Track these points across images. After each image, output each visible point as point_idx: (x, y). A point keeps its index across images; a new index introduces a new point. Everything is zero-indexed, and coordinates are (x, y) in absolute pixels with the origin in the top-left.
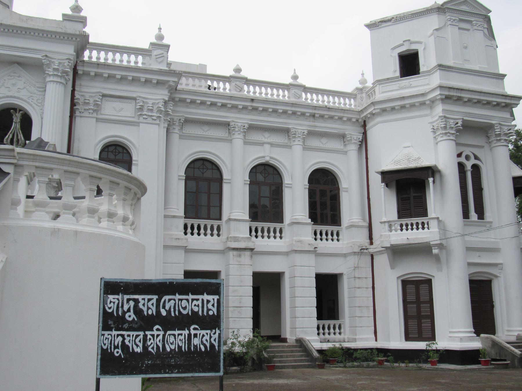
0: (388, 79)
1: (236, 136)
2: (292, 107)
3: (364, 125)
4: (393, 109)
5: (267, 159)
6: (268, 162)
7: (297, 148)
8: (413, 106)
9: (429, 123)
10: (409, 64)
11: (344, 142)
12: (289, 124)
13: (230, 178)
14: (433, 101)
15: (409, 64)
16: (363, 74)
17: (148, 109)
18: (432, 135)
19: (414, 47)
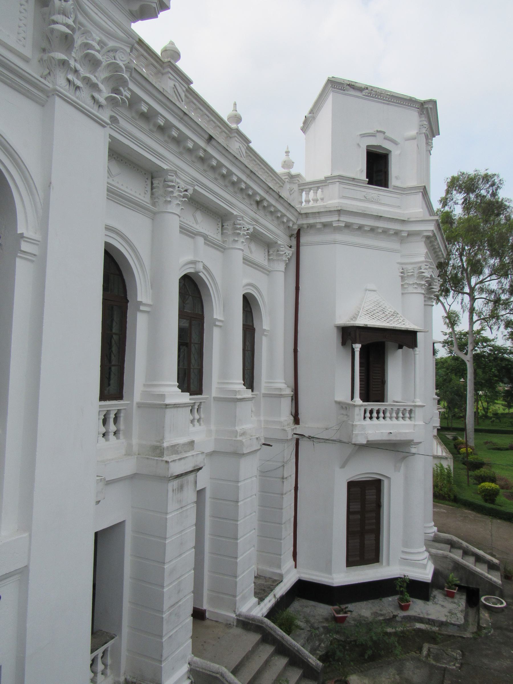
0: (354, 179)
1: (174, 207)
2: (248, 176)
3: (298, 236)
4: (360, 227)
5: (200, 267)
6: (196, 274)
7: (237, 256)
8: (385, 232)
9: (398, 263)
10: (377, 167)
11: (269, 255)
12: (231, 204)
13: (150, 302)
14: (411, 234)
15: (377, 167)
16: (287, 152)
17: (87, 55)
18: (399, 282)
19: (387, 145)
